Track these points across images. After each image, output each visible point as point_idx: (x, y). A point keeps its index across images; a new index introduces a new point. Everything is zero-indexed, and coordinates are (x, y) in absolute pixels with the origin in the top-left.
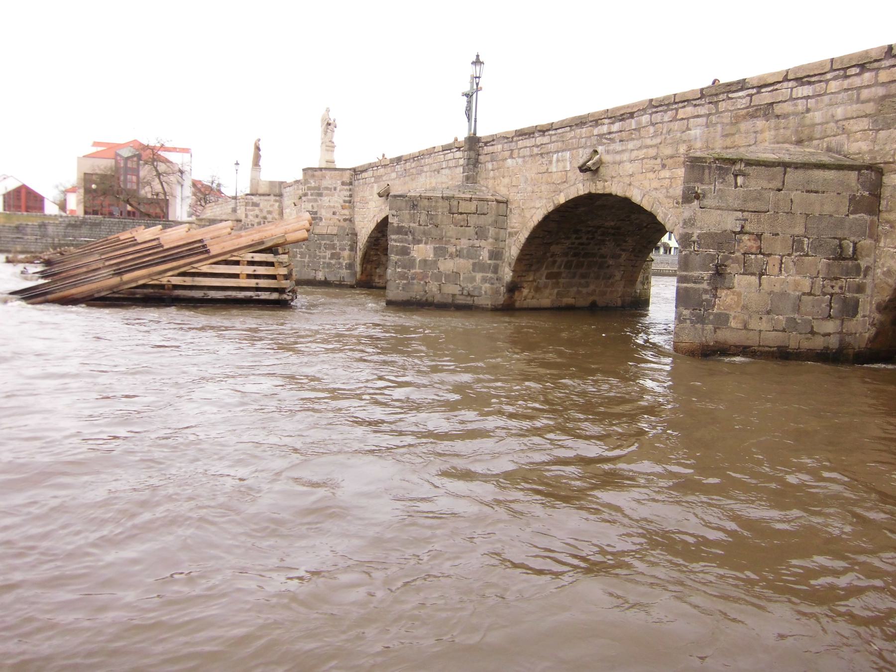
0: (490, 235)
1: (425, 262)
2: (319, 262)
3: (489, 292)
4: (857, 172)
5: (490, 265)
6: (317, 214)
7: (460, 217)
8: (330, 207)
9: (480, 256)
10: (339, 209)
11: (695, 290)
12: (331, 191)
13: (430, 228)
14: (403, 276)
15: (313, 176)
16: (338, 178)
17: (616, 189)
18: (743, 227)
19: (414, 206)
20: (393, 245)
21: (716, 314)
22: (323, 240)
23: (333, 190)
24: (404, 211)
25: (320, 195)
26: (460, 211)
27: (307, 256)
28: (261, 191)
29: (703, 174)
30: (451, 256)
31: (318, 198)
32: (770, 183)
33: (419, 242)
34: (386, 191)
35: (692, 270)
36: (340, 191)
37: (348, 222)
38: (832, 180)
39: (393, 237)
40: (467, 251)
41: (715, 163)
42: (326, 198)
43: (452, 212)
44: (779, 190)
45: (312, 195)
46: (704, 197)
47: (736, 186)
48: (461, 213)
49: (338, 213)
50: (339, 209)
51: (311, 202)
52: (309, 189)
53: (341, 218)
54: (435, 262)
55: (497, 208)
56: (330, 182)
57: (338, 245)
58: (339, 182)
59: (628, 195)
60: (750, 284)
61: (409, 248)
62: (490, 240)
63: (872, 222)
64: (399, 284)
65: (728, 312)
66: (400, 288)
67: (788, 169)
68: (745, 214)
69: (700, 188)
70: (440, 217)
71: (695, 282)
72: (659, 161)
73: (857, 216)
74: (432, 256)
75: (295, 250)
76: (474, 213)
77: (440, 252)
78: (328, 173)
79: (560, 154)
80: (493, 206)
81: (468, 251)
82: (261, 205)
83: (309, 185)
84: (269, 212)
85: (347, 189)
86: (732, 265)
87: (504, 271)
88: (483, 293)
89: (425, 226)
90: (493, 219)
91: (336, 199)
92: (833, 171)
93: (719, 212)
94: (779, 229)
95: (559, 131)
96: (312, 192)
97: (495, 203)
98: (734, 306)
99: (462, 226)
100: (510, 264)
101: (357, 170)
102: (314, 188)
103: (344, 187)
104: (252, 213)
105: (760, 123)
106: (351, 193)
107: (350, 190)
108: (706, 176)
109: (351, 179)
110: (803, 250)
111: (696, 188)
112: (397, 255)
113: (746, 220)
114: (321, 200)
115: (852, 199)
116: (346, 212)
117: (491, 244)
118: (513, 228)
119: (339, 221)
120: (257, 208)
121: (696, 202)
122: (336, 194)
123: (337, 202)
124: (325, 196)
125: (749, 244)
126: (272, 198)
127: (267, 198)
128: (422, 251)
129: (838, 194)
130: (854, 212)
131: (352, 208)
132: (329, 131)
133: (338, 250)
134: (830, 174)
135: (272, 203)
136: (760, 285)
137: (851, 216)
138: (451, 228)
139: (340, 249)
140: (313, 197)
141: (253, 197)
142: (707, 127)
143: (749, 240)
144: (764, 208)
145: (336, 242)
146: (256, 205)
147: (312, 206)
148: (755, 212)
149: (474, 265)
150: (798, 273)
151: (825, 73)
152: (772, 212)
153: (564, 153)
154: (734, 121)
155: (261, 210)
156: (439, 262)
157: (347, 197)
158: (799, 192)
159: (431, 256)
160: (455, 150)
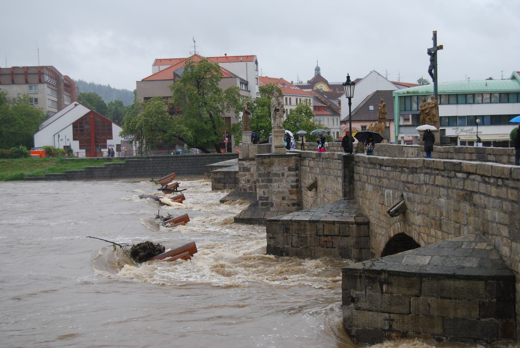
0: (353, 256)
4: (483, 282)
6: (268, 200)
7: (325, 239)
10: (287, 194)
12: (279, 177)
15: (263, 163)
16: (285, 164)
18: (390, 326)
19: (287, 230)
23: (281, 175)
25: (270, 181)
26: (325, 233)
28: (251, 156)
29: (356, 282)
31: (269, 184)
32: (409, 290)
36: (287, 177)
38: (462, 288)
41: (364, 274)
42: (275, 184)
43: (318, 234)
44: (419, 296)
45: (262, 181)
46: (358, 300)
47: (382, 292)
48: (327, 236)
49: (287, 198)
50: (287, 194)
53: (289, 203)
56: (278, 169)
67: (424, 279)
68: (392, 315)
69: (354, 293)
70: (309, 238)
76: (337, 236)
78: (276, 160)
80: (354, 228)
83: (260, 172)
85: (293, 175)
89: (296, 247)
90: (355, 240)
92: (462, 281)
93: (371, 313)
94: (421, 329)
97: (355, 225)
99: (327, 248)
101: (303, 155)
106: (297, 178)
107: (297, 175)
108: (359, 285)
109: (297, 164)
111: (352, 293)
113: (393, 320)
114: (271, 186)
115: (482, 305)
116: (294, 197)
119: (289, 205)
121: (352, 305)
122: (284, 180)
123: (285, 187)
124: (274, 183)
129: (469, 300)
130: (483, 317)
132: (277, 116)
134: (460, 284)
137: (482, 320)
138: (318, 249)
141: (244, 162)
142: (448, 199)
143: (397, 336)
144: (405, 311)
147: (264, 192)
148: (399, 314)
151: (489, 177)
152: (413, 315)
154: (458, 200)
155: (252, 175)
157: (294, 182)
158: (435, 298)
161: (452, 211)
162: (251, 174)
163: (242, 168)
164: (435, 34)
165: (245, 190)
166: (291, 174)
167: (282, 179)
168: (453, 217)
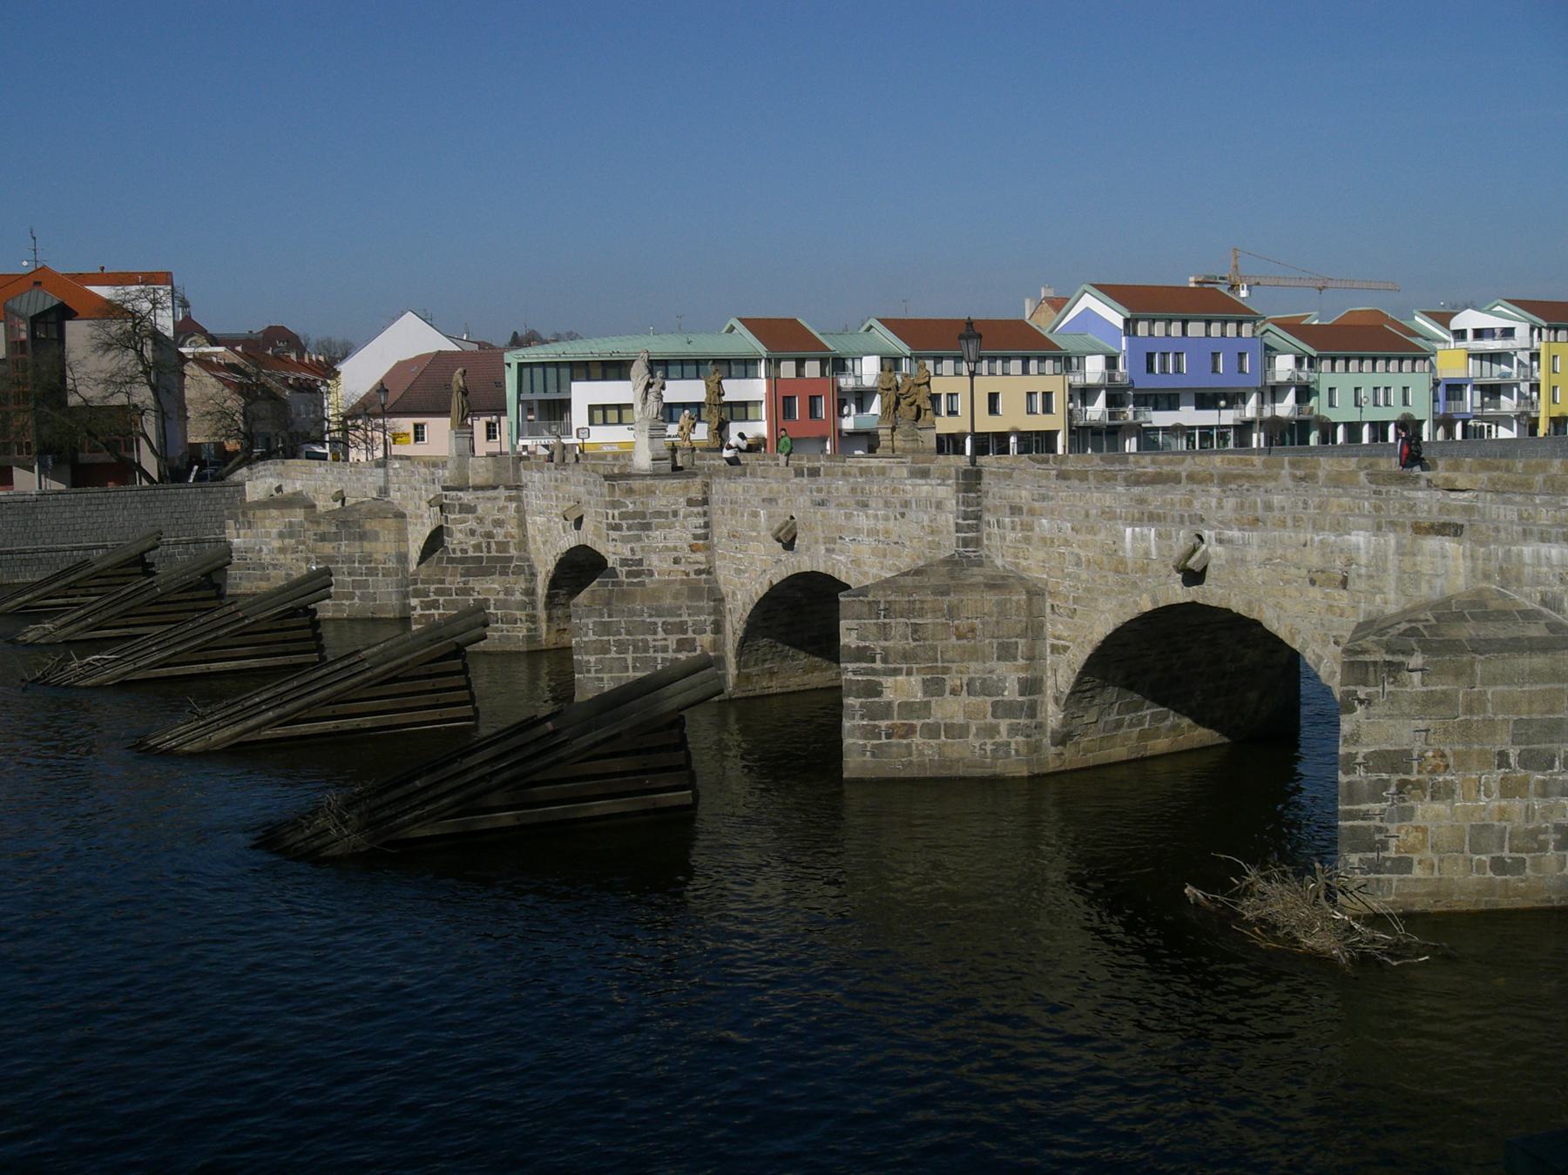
1: (908, 708)
2: (656, 658)
3: (1023, 750)
8: (667, 548)
9: (1003, 691)
11: (1367, 829)
13: (916, 647)
14: (873, 733)
15: (630, 491)
17: (1237, 605)
21: (1393, 860)
22: (659, 616)
23: (670, 516)
24: (866, 621)
25: (647, 527)
27: (631, 648)
29: (1367, 672)
30: (954, 692)
33: (896, 672)
36: (685, 517)
37: (704, 576)
39: (851, 666)
40: (981, 684)
45: (629, 528)
49: (683, 560)
51: (629, 542)
53: (691, 569)
54: (927, 704)
56: (665, 503)
57: (690, 624)
59: (1255, 616)
60: (1438, 816)
61: (880, 684)
62: (1021, 662)
64: (865, 745)
65: (1410, 855)
66: (868, 753)
70: (930, 627)
71: (1363, 819)
72: (1304, 572)
74: (919, 695)
75: (606, 638)
77: (934, 686)
79: (1137, 529)
80: (1022, 603)
82: (480, 510)
83: (624, 510)
84: (498, 523)
86: (1413, 792)
87: (1046, 711)
88: (1013, 752)
91: (680, 534)
95: (1136, 490)
96: (631, 522)
98: (1419, 847)
100: (1056, 700)
102: (634, 515)
103: (692, 509)
104: (461, 526)
105: (1450, 545)
106: (706, 519)
107: (705, 514)
108: (1371, 678)
109: (705, 493)
110: (1508, 766)
112: (858, 697)
113: (1427, 731)
114: (648, 537)
116: (700, 557)
117: (1026, 668)
118: (1059, 639)
122: (677, 524)
123: (680, 538)
124: (657, 530)
125: (1434, 762)
126: (502, 493)
127: (490, 493)
131: (708, 548)
133: (690, 635)
134: (1539, 661)
135: (502, 503)
136: (1454, 814)
139: (694, 632)
140: (631, 533)
141: (460, 494)
145: (685, 618)
146: (468, 509)
147: (632, 550)
149: (995, 705)
150: (1503, 796)
153: (1146, 530)
155: (480, 520)
156: (933, 705)
157: (700, 527)
159: (920, 696)
160: (934, 482)
162: (478, 518)
163: (458, 507)
165: (464, 551)
166: (692, 512)
167: (673, 523)
168: (1392, 561)
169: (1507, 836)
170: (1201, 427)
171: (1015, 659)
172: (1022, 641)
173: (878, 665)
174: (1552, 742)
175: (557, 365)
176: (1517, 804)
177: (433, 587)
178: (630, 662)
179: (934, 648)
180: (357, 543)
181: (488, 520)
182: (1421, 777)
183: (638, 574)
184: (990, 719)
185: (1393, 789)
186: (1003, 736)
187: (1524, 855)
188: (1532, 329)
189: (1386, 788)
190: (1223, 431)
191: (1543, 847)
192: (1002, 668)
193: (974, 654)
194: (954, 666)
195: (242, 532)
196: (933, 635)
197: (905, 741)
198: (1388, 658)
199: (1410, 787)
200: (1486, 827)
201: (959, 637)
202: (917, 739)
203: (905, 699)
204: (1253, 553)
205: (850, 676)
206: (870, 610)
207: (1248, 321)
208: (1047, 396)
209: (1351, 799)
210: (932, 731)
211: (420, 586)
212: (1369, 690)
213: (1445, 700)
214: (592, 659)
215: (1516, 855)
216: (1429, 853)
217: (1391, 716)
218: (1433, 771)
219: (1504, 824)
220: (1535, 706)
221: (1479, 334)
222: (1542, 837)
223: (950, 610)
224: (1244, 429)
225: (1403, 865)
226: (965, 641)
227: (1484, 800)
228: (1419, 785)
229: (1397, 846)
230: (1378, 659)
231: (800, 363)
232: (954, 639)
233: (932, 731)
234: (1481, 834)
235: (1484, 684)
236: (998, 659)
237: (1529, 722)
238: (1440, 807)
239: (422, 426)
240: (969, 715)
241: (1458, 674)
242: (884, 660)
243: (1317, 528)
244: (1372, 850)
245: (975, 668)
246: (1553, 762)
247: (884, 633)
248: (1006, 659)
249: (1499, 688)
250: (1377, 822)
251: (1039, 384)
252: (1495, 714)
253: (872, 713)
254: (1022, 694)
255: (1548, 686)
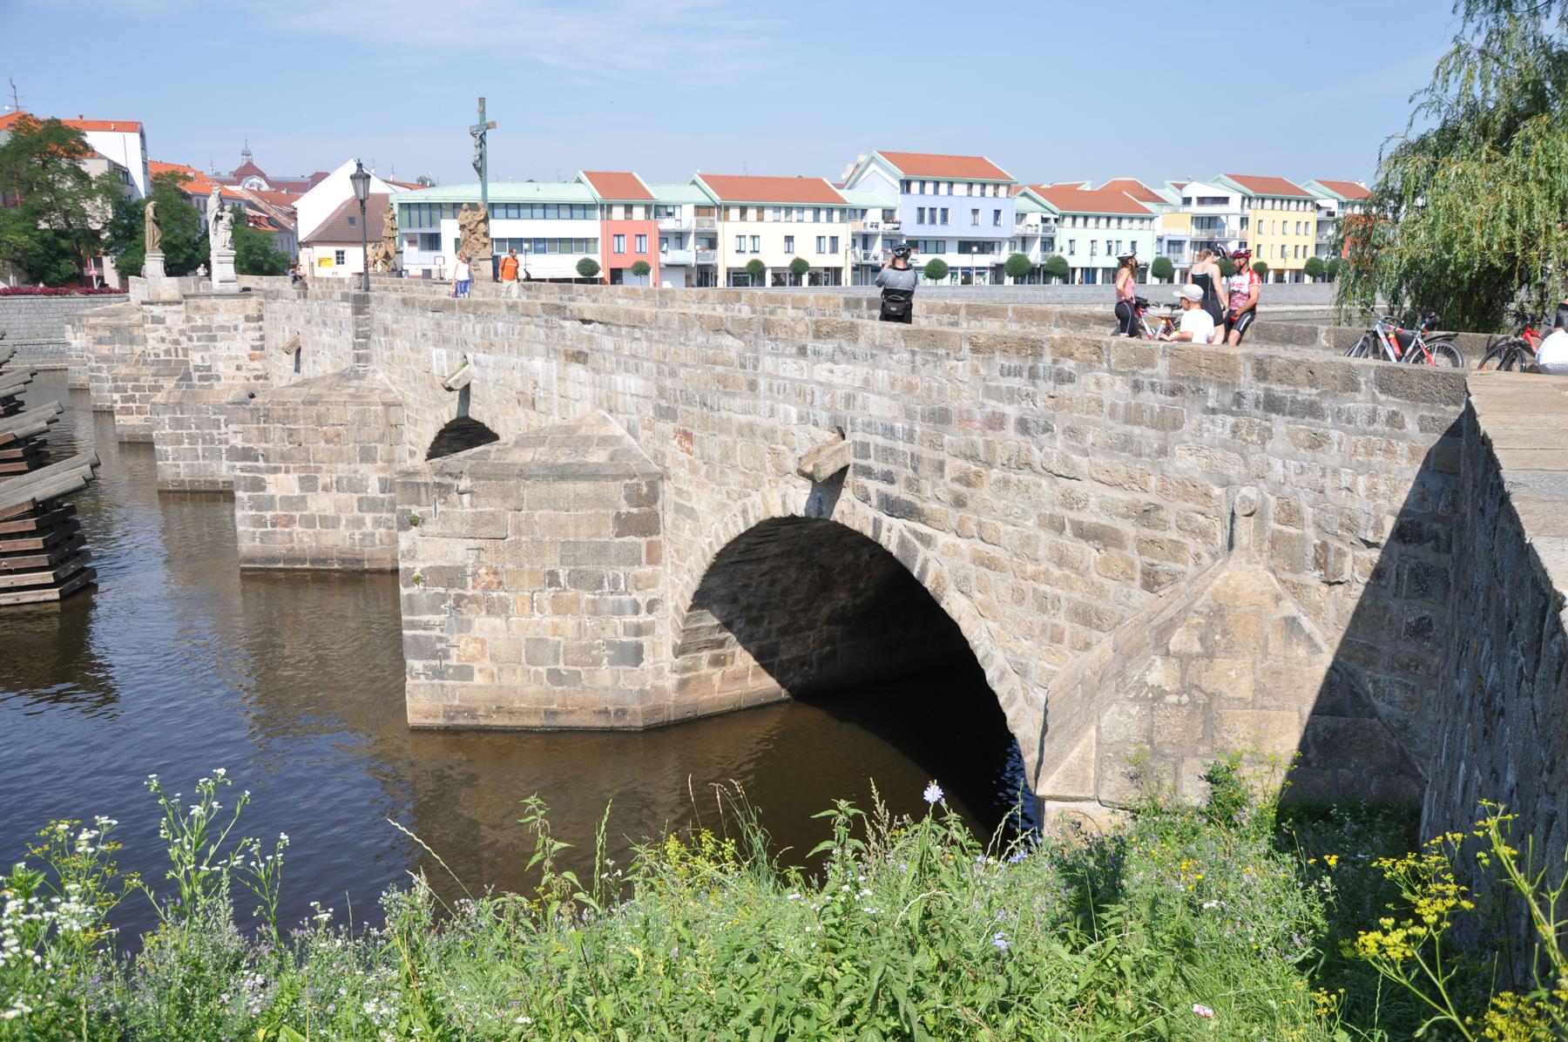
0: (378, 457)
1: (288, 501)
3: (387, 540)
5: (383, 500)
8: (231, 358)
10: (245, 361)
11: (429, 638)
14: (259, 522)
15: (198, 308)
16: (239, 310)
20: (240, 477)
21: (456, 668)
25: (213, 339)
28: (165, 297)
29: (419, 494)
30: (326, 489)
31: (211, 344)
33: (276, 470)
34: (292, 345)
35: (420, 614)
37: (261, 381)
45: (199, 339)
50: (245, 361)
52: (194, 329)
54: (303, 499)
55: (387, 414)
56: (226, 317)
58: (241, 317)
60: (494, 630)
61: (263, 480)
62: (380, 464)
63: (649, 544)
64: (254, 533)
69: (416, 511)
70: (303, 432)
71: (424, 629)
73: (625, 539)
77: (308, 483)
81: (350, 480)
82: (168, 322)
93: (445, 540)
102: (202, 328)
104: (154, 335)
107: (260, 329)
108: (423, 497)
110: (559, 584)
112: (246, 491)
113: (478, 549)
116: (257, 364)
119: (248, 379)
120: (161, 326)
123: (241, 349)
125: (487, 579)
128: (282, 484)
134: (583, 487)
136: (508, 629)
137: (617, 540)
141: (152, 307)
146: (159, 320)
147: (202, 358)
149: (360, 500)
150: (556, 612)
155: (169, 330)
159: (297, 492)
161: (555, 380)
164: (482, 101)
165: (157, 355)
168: (555, 388)
169: (562, 650)
170: (963, 268)
171: (374, 461)
172: (380, 446)
173: (261, 464)
174: (599, 563)
175: (430, 205)
176: (569, 623)
177: (130, 385)
178: (200, 451)
179: (307, 450)
180: (128, 347)
181: (175, 330)
182: (475, 592)
183: (207, 378)
184: (356, 513)
185: (450, 602)
186: (369, 528)
187: (579, 668)
188: (1243, 199)
189: (444, 602)
190: (981, 271)
191: (597, 662)
192: (364, 468)
193: (340, 457)
194: (324, 467)
195: (78, 335)
196: (306, 439)
197: (287, 530)
198: (437, 480)
199: (466, 601)
200: (539, 642)
201: (328, 441)
202: (297, 528)
203: (285, 494)
204: (491, 375)
205: (238, 473)
206: (252, 416)
207: (1004, 184)
208: (834, 239)
209: (412, 611)
210: (309, 522)
211: (120, 383)
212: (424, 509)
213: (493, 519)
214: (170, 449)
215: (572, 668)
216: (487, 663)
217: (444, 536)
218: (487, 588)
219: (558, 638)
220: (582, 530)
221: (1202, 200)
222: (595, 652)
223: (319, 416)
224: (998, 271)
225: (464, 673)
226: (331, 446)
227: (537, 616)
228: (473, 599)
229: (458, 655)
230: (429, 480)
231: (629, 208)
232: (322, 444)
233: (309, 522)
234: (535, 649)
235: (530, 509)
236: (361, 461)
237: (576, 544)
238: (498, 622)
239: (343, 253)
240: (339, 509)
241: (505, 497)
242: (266, 460)
243: (520, 354)
244: (434, 657)
245: (342, 469)
246: (601, 582)
247: (264, 435)
248: (367, 461)
249: (545, 512)
250: (436, 632)
251: (827, 229)
252: (544, 536)
253: (260, 505)
254: (383, 492)
255: (593, 511)
